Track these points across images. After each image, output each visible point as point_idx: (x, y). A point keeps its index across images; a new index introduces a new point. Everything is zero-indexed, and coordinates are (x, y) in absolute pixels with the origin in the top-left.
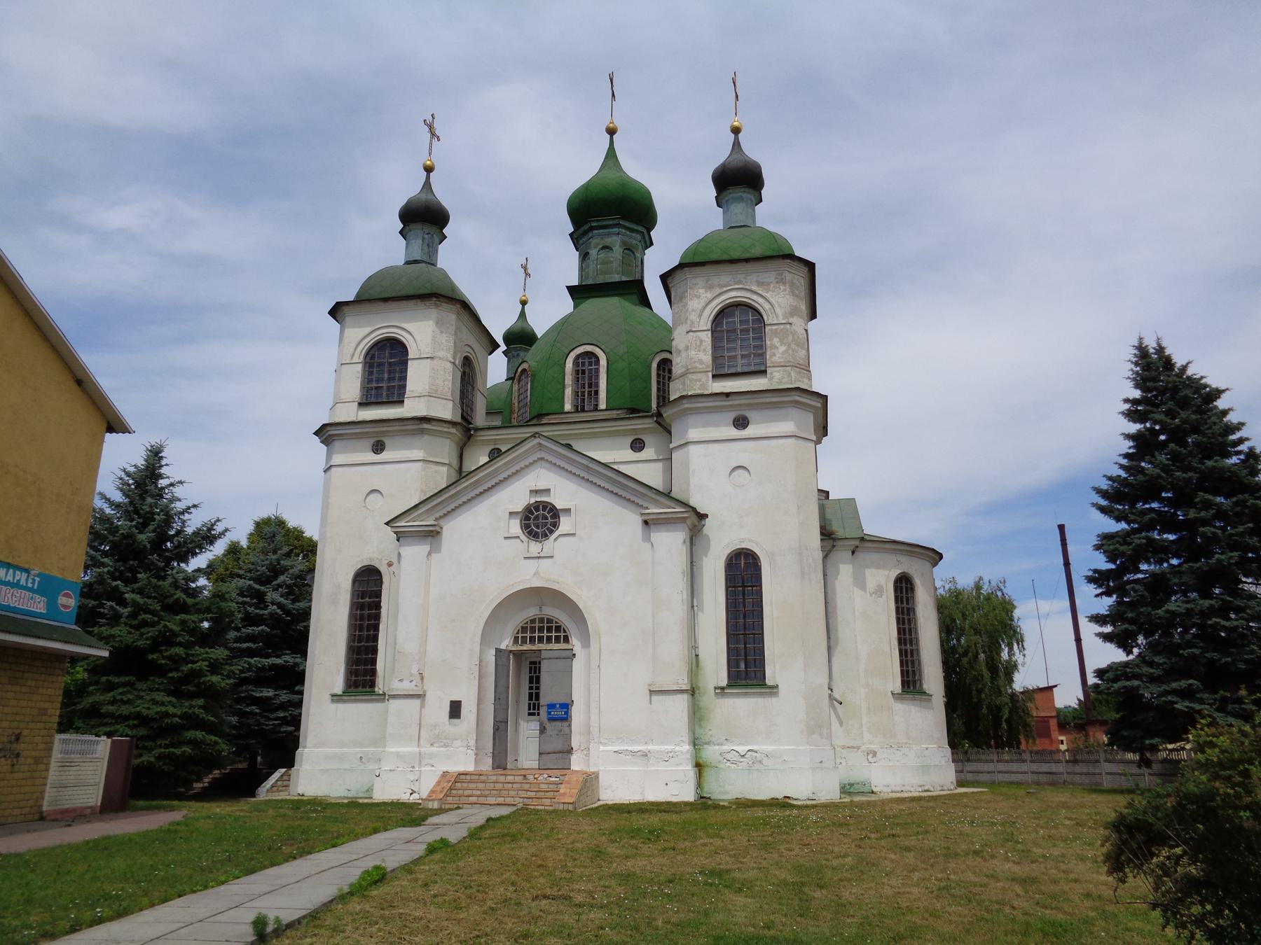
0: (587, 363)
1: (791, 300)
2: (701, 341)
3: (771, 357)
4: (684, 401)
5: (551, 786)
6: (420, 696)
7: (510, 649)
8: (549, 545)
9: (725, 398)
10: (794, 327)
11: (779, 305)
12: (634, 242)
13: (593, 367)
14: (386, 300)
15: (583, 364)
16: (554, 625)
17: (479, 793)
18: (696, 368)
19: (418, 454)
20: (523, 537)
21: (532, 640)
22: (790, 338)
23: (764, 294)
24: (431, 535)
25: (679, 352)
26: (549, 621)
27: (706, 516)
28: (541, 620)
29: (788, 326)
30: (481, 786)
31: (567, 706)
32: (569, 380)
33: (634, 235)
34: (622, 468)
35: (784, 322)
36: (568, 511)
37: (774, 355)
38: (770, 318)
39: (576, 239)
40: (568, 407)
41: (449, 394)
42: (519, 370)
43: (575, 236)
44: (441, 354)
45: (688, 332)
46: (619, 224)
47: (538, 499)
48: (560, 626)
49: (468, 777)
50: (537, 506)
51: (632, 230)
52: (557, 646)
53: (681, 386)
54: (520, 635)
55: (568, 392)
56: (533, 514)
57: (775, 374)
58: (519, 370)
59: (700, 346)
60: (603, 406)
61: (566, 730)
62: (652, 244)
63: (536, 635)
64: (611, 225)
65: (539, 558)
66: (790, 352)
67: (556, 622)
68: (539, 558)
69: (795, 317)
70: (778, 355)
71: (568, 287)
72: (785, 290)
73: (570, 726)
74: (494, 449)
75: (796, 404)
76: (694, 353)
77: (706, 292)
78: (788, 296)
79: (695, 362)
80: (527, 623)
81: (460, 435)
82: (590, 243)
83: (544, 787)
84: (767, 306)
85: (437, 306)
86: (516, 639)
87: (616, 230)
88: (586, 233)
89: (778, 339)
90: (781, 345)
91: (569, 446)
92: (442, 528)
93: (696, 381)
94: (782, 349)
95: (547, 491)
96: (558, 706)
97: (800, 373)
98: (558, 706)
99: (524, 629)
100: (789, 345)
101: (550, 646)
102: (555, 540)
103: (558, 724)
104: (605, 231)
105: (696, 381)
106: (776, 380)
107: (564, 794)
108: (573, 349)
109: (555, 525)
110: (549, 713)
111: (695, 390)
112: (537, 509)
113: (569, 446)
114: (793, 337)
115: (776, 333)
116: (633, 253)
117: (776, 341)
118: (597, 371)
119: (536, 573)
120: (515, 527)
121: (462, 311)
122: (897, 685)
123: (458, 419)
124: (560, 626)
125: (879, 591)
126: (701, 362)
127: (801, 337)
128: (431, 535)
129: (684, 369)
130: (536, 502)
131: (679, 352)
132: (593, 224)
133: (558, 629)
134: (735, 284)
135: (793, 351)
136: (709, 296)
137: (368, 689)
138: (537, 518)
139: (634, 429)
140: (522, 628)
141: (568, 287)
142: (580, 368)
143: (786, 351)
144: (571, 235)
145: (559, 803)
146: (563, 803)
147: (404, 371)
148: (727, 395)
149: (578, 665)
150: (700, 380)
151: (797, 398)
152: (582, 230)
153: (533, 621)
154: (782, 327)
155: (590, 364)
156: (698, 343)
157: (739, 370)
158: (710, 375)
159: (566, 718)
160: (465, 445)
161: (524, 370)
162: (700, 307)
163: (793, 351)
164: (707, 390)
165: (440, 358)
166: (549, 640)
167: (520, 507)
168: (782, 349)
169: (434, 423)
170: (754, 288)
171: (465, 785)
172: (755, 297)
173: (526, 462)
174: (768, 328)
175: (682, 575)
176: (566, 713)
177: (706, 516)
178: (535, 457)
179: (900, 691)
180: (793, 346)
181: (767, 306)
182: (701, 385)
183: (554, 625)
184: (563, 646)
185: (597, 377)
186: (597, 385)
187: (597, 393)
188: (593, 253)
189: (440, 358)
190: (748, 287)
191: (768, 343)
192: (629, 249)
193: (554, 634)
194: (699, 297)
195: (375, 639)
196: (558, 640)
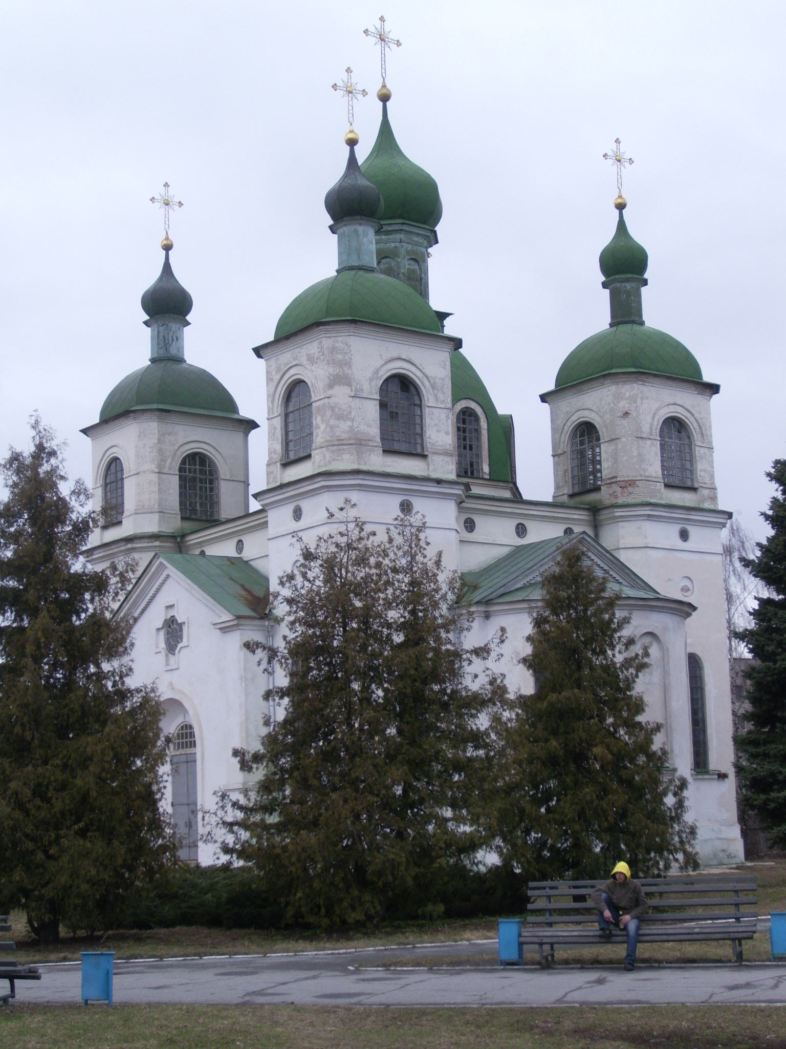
1: (331, 370)
10: (331, 400)
12: (393, 245)
20: (163, 653)
29: (326, 400)
36: (184, 623)
37: (317, 436)
70: (320, 435)
78: (326, 367)
97: (340, 450)
106: (316, 464)
109: (181, 638)
114: (332, 410)
117: (319, 418)
127: (344, 407)
135: (331, 427)
136: (279, 377)
143: (326, 428)
147: (122, 487)
158: (278, 464)
163: (331, 427)
164: (277, 482)
168: (323, 427)
173: (160, 581)
174: (314, 405)
178: (164, 576)
180: (332, 422)
189: (145, 472)
191: (314, 422)
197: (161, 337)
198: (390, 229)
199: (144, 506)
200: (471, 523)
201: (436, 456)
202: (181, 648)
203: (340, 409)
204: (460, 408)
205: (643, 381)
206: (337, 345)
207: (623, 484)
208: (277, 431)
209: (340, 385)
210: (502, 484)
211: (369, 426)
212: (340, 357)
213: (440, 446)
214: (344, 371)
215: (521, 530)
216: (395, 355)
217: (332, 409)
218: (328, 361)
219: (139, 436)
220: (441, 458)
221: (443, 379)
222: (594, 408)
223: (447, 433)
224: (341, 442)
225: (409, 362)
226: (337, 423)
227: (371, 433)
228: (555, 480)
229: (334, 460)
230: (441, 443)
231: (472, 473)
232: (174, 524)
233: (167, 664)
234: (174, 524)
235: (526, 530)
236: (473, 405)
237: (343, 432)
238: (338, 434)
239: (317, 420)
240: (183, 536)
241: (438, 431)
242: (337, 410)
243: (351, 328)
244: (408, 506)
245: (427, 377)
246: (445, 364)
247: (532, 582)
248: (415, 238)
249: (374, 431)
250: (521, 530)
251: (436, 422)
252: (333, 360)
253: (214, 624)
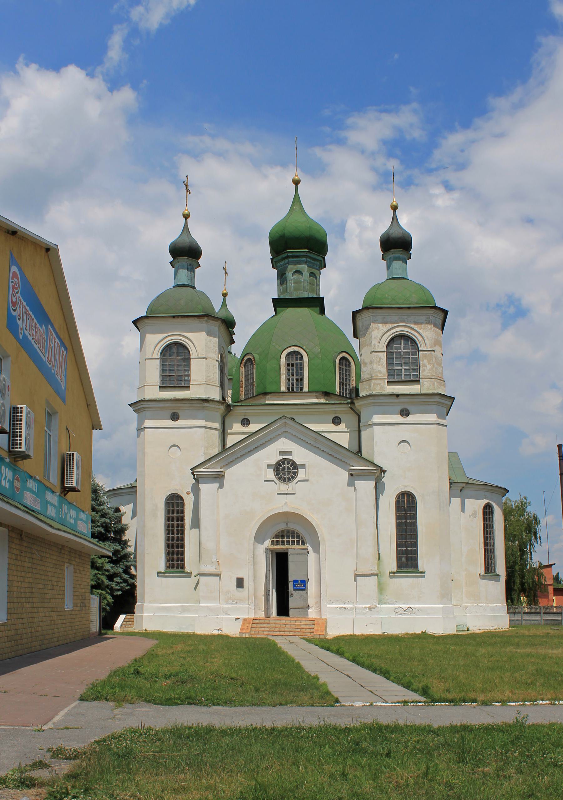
0: (295, 359)
2: (380, 358)
3: (422, 372)
4: (371, 398)
5: (307, 626)
6: (218, 575)
7: (270, 548)
8: (292, 486)
9: (396, 397)
11: (427, 338)
13: (299, 362)
15: (292, 359)
16: (295, 534)
17: (268, 629)
18: (377, 376)
19: (202, 423)
20: (276, 481)
21: (283, 543)
22: (434, 360)
23: (418, 330)
24: (219, 478)
25: (365, 364)
26: (293, 532)
27: (386, 471)
28: (288, 531)
30: (267, 625)
31: (304, 582)
32: (283, 369)
33: (315, 262)
34: (327, 435)
35: (431, 350)
36: (303, 466)
37: (424, 370)
38: (422, 346)
39: (275, 262)
40: (283, 388)
42: (245, 358)
43: (275, 260)
45: (372, 352)
46: (307, 255)
47: (285, 457)
48: (299, 535)
49: (258, 621)
50: (283, 461)
51: (314, 259)
52: (298, 547)
53: (367, 387)
54: (275, 540)
55: (283, 378)
56: (281, 466)
57: (425, 383)
58: (245, 358)
59: (379, 362)
60: (306, 389)
61: (305, 596)
62: (325, 267)
63: (285, 540)
64: (302, 256)
65: (287, 494)
66: (434, 369)
67: (297, 533)
68: (287, 494)
69: (437, 346)
70: (427, 371)
71: (272, 299)
72: (431, 329)
73: (307, 593)
74: (244, 419)
75: (438, 403)
76: (375, 366)
77: (383, 326)
79: (376, 372)
80: (279, 533)
81: (224, 410)
82: (287, 267)
83: (303, 626)
84: (420, 338)
86: (273, 542)
87: (304, 259)
88: (284, 259)
89: (427, 361)
90: (429, 364)
91: (293, 419)
92: (225, 473)
93: (378, 384)
94: (429, 367)
95: (290, 453)
96: (299, 582)
98: (299, 582)
99: (277, 537)
100: (433, 366)
101: (294, 547)
102: (296, 483)
103: (300, 592)
104: (297, 259)
105: (378, 384)
106: (425, 387)
107: (317, 630)
108: (285, 349)
110: (294, 586)
111: (377, 390)
112: (284, 463)
113: (293, 419)
115: (425, 356)
116: (315, 275)
117: (425, 361)
118: (302, 364)
119: (286, 504)
120: (271, 474)
123: (221, 399)
124: (299, 535)
126: (380, 372)
128: (219, 478)
129: (369, 376)
130: (283, 459)
131: (365, 364)
132: (290, 254)
133: (298, 537)
134: (401, 322)
135: (436, 368)
137: (180, 569)
138: (284, 469)
139: (335, 411)
140: (276, 535)
141: (272, 299)
142: (290, 362)
144: (271, 259)
145: (317, 635)
146: (320, 635)
148: (398, 396)
149: (312, 557)
150: (379, 384)
152: (280, 257)
153: (283, 532)
154: (429, 352)
155: (297, 360)
156: (378, 359)
157: (403, 379)
158: (386, 381)
159: (304, 589)
160: (226, 415)
161: (249, 360)
162: (380, 336)
163: (436, 368)
164: (384, 391)
166: (293, 543)
167: (273, 462)
168: (429, 367)
170: (412, 326)
171: (258, 625)
172: (413, 332)
175: (373, 507)
176: (305, 586)
177: (386, 471)
180: (436, 365)
181: (420, 338)
182: (381, 388)
183: (295, 534)
184: (301, 547)
185: (302, 369)
186: (302, 374)
187: (301, 379)
188: (289, 274)
190: (409, 325)
191: (421, 362)
192: (312, 275)
193: (295, 540)
194: (378, 329)
195: (183, 539)
196: (298, 543)
202: (299, 481)
203: (438, 359)
208: (382, 360)
218: (433, 330)
237: (439, 373)
238: (438, 373)
239: (423, 361)
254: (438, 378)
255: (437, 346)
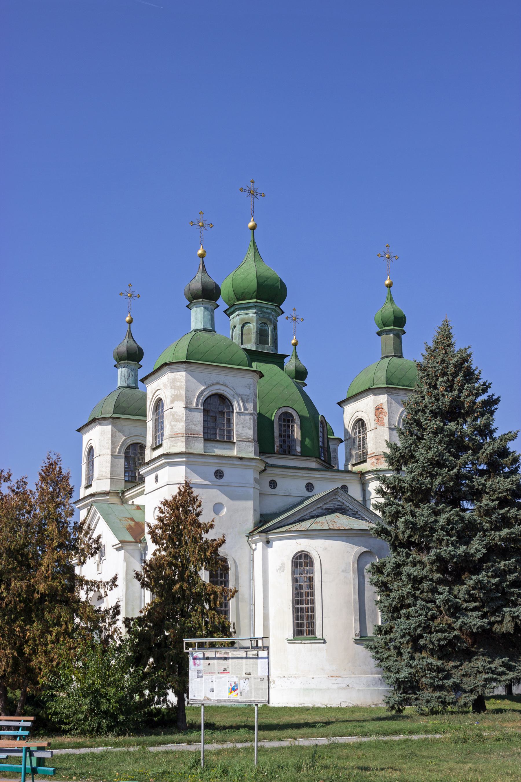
1: (173, 392)
12: (251, 315)
14: (87, 425)
41: (109, 475)
44: (104, 452)
75: (170, 464)
78: (170, 390)
85: (100, 424)
121: (115, 421)
122: (289, 633)
125: (282, 568)
127: (180, 414)
135: (172, 426)
151: (165, 461)
165: (104, 455)
169: (96, 496)
179: (292, 638)
180: (173, 423)
189: (104, 455)
197: (123, 374)
198: (249, 305)
199: (102, 475)
200: (274, 483)
201: (241, 442)
204: (281, 412)
205: (392, 392)
206: (177, 377)
207: (377, 457)
209: (177, 400)
210: (309, 458)
211: (195, 425)
212: (178, 384)
213: (244, 436)
214: (180, 392)
215: (310, 487)
216: (215, 382)
217: (173, 415)
218: (171, 386)
219: (101, 434)
220: (244, 443)
221: (248, 396)
222: (364, 410)
223: (249, 428)
224: (177, 435)
225: (225, 385)
226: (175, 423)
227: (197, 430)
228: (346, 455)
229: (173, 446)
230: (245, 435)
231: (289, 452)
232: (121, 486)
233: (98, 570)
234: (121, 486)
235: (313, 487)
236: (290, 411)
240: (123, 493)
241: (243, 427)
242: (175, 416)
243: (184, 365)
244: (220, 473)
245: (237, 394)
246: (250, 386)
247: (301, 519)
248: (266, 310)
249: (199, 428)
250: (310, 487)
251: (242, 422)
252: (174, 386)
253: (113, 546)
254: (174, 436)
255: (176, 402)
